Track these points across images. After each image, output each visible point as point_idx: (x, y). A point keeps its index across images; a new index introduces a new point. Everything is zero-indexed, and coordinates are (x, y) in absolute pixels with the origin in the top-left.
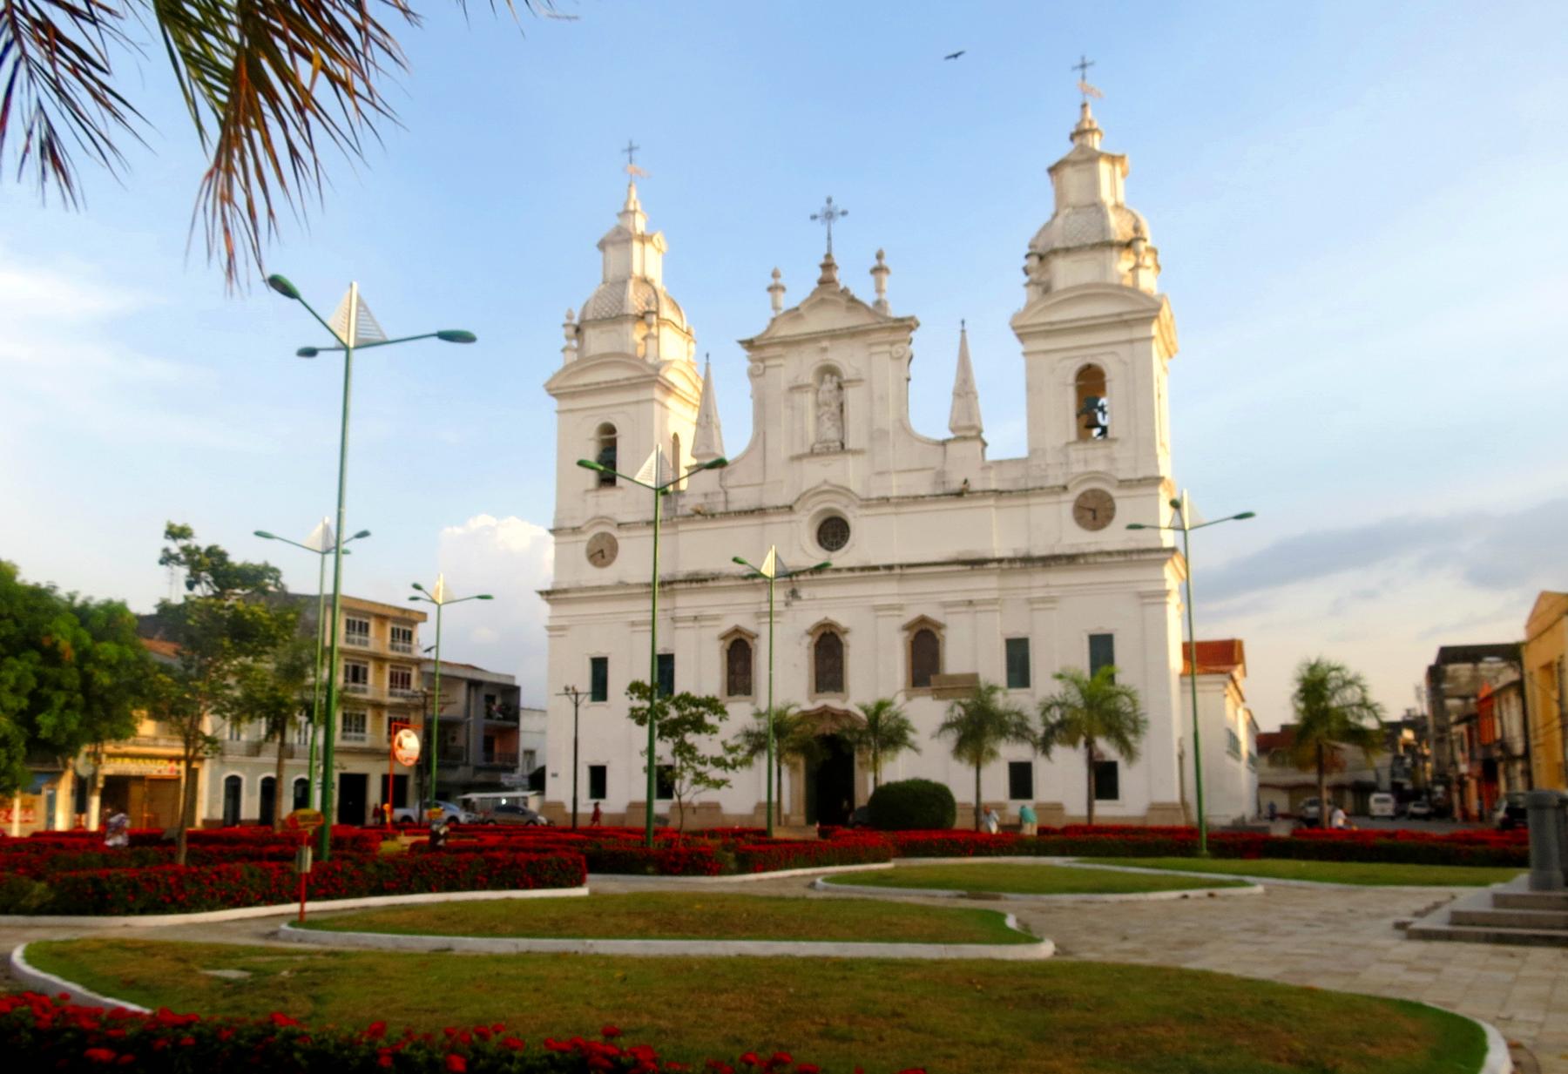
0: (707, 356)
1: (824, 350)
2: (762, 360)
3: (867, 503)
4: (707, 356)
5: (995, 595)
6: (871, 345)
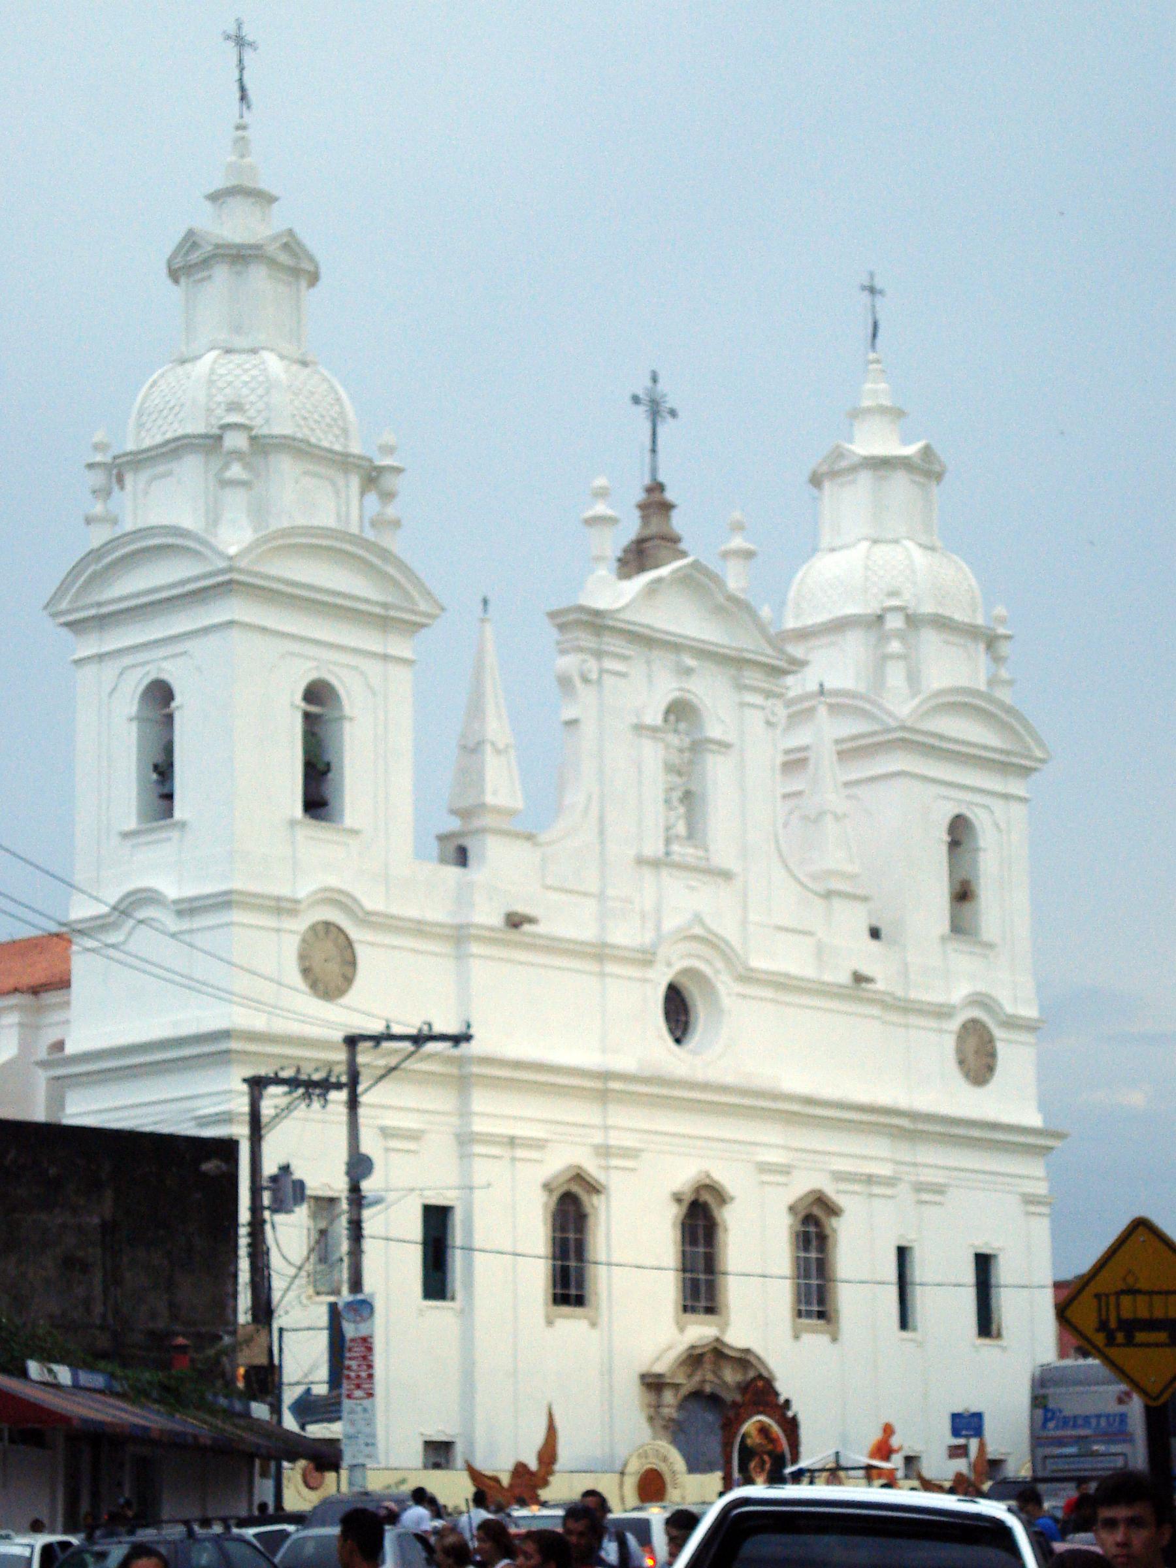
0: (485, 602)
1: (688, 671)
2: (599, 654)
3: (748, 977)
4: (485, 602)
5: (885, 1170)
6: (741, 687)
